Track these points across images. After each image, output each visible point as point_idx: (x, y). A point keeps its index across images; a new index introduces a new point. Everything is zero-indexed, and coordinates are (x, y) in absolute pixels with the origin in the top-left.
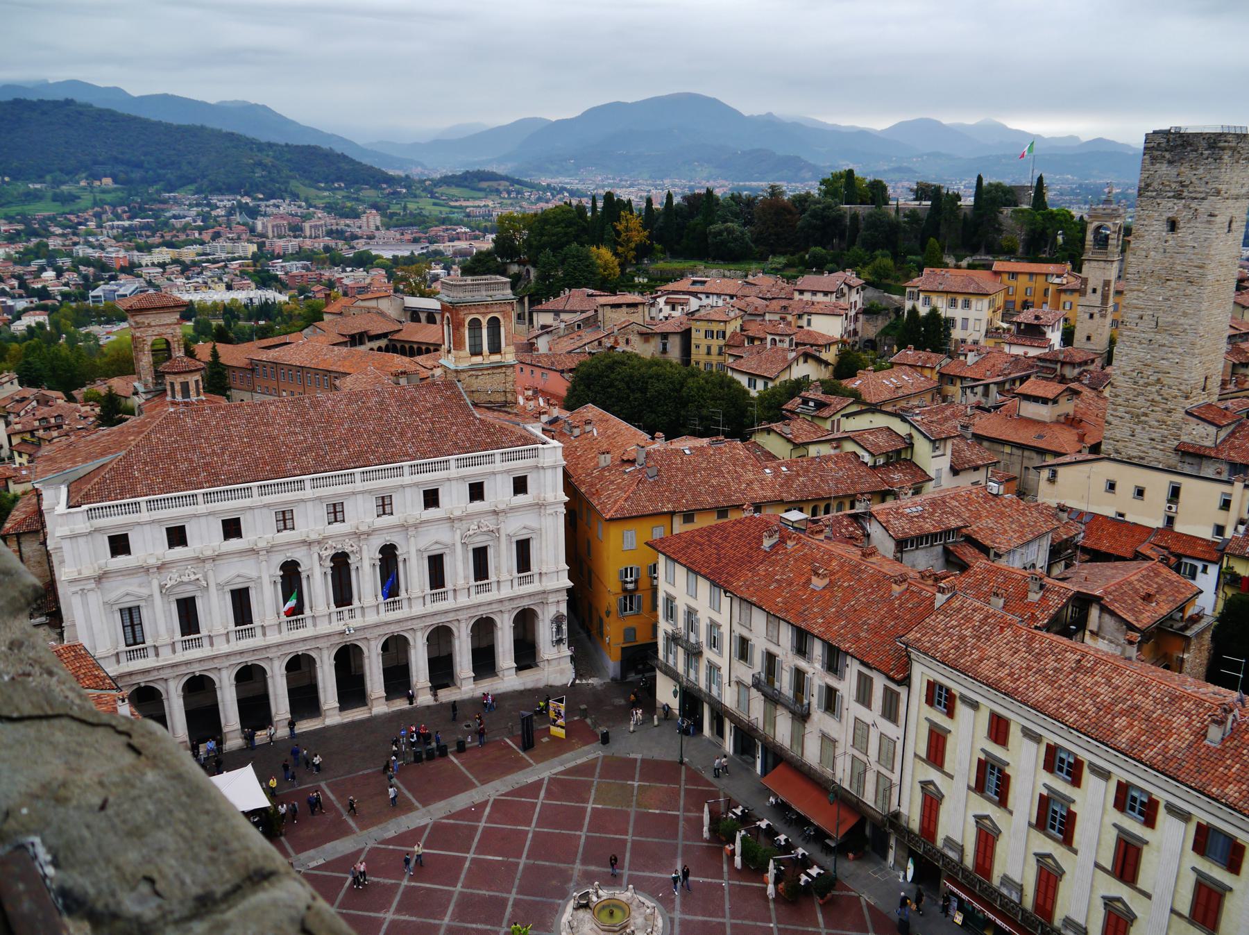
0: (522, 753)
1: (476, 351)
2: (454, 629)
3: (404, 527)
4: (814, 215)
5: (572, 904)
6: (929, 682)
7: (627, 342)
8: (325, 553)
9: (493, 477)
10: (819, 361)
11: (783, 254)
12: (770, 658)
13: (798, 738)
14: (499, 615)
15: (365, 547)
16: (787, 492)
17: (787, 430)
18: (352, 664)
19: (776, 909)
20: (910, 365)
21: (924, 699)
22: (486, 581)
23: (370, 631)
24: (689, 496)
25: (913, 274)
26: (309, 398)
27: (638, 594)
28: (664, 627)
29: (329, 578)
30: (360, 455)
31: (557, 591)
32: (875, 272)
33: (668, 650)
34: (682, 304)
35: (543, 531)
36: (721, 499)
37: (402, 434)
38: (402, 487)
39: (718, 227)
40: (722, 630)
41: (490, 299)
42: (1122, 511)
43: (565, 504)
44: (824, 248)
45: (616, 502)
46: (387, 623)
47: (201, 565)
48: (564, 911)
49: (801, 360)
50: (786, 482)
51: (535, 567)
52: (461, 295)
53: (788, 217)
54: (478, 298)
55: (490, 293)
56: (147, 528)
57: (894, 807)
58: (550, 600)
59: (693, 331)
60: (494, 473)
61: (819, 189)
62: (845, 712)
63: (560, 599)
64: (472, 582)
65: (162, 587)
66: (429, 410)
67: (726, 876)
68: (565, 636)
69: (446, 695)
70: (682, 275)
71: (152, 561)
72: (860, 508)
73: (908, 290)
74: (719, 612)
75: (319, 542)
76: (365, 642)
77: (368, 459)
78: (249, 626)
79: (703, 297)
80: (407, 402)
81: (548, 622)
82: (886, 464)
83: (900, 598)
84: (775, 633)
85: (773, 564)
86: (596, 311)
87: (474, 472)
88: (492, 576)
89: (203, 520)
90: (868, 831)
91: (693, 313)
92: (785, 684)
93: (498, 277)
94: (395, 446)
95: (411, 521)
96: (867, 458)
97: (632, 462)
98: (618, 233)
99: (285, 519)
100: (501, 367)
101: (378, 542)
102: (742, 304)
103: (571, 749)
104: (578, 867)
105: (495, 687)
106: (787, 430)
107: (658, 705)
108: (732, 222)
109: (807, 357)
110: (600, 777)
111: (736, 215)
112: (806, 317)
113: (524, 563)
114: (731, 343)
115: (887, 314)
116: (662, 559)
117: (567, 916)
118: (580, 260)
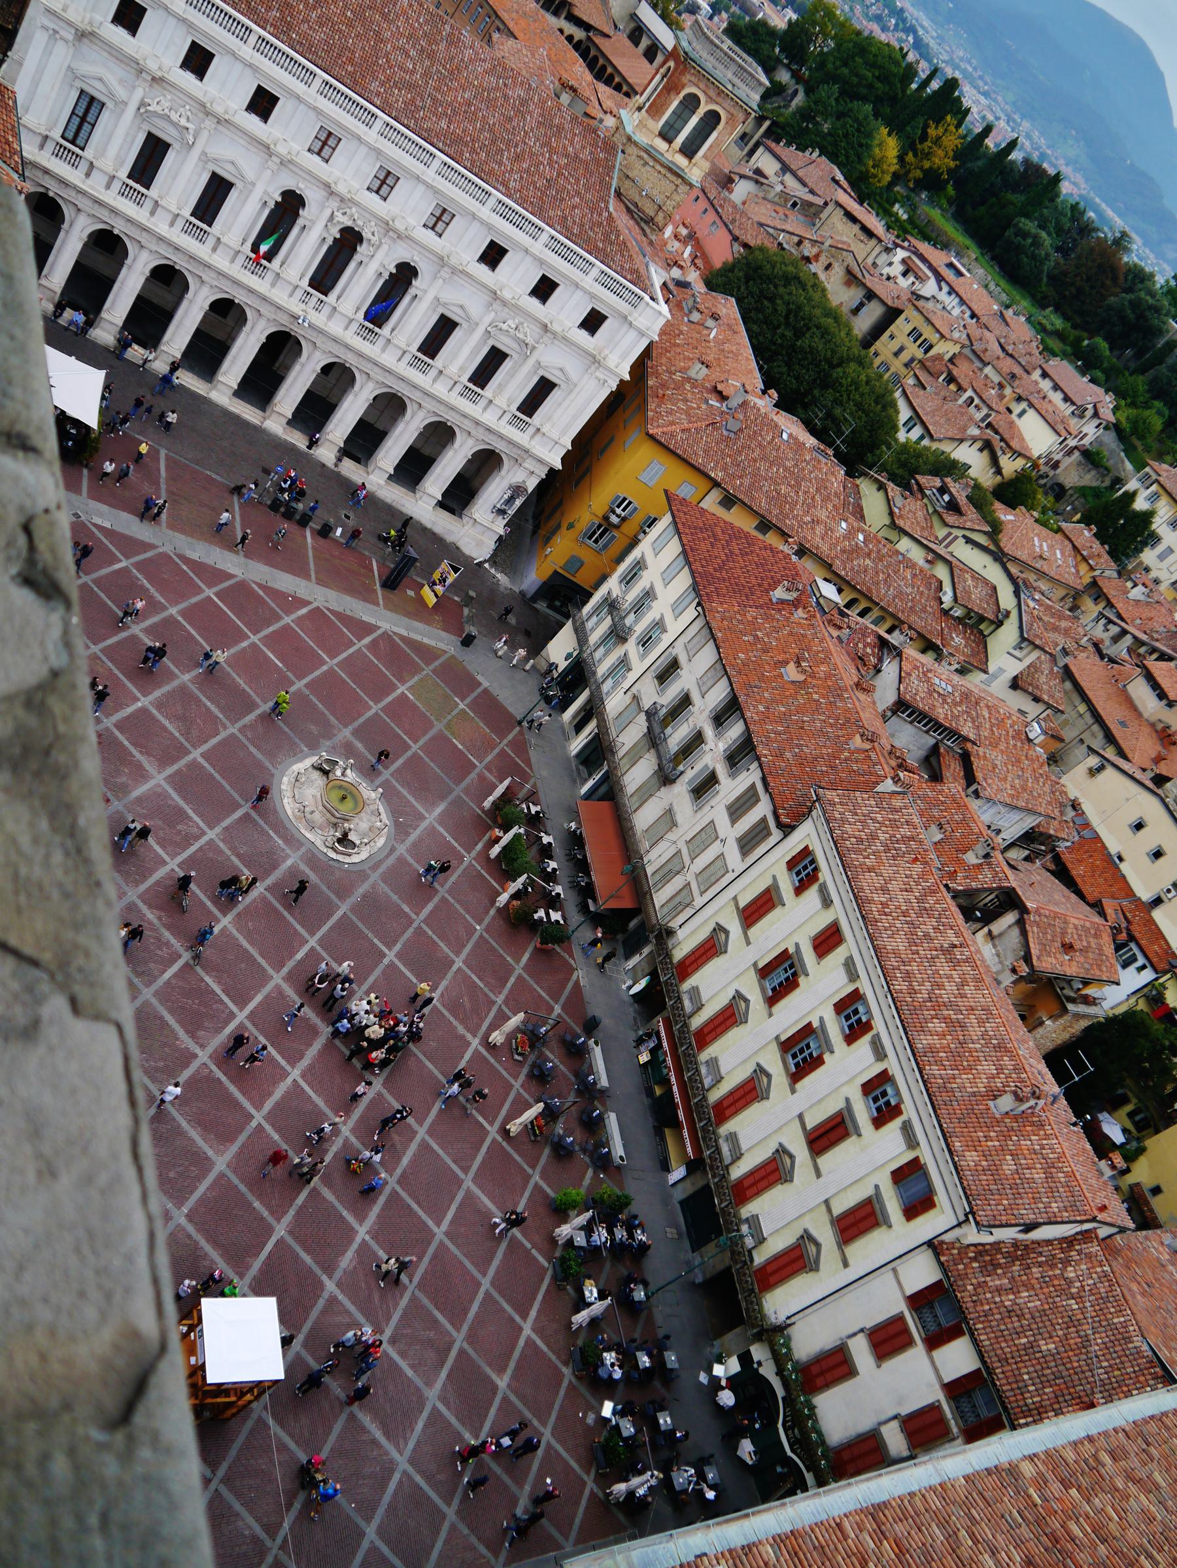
0: (378, 587)
1: (667, 135)
3: (442, 261)
4: (1136, 305)
5: (314, 759)
6: (807, 847)
7: (828, 267)
8: (339, 217)
9: (573, 288)
10: (995, 461)
11: (1066, 318)
12: (685, 701)
13: (645, 793)
14: (465, 435)
15: (385, 247)
16: (843, 562)
17: (899, 501)
18: (281, 358)
19: (494, 918)
20: (1074, 547)
21: (788, 858)
22: (478, 390)
23: (324, 339)
24: (747, 481)
25: (1169, 458)
26: (452, 27)
27: (615, 533)
28: (612, 585)
30: (457, 140)
31: (540, 461)
32: (1134, 422)
33: (597, 610)
34: (917, 277)
36: (775, 512)
37: (518, 158)
38: (474, 216)
39: (1029, 225)
40: (664, 636)
41: (730, 87)
42: (1124, 856)
43: (622, 381)
44: (1111, 349)
45: (672, 423)
46: (347, 347)
47: (201, 115)
48: (301, 760)
49: (978, 444)
50: (852, 552)
52: (705, 55)
53: (1108, 282)
54: (718, 74)
55: (736, 80)
56: (172, 21)
57: (674, 924)
58: (526, 465)
59: (903, 317)
60: (577, 286)
61: (1167, 281)
62: (707, 808)
64: (464, 379)
65: (143, 104)
66: (567, 156)
67: (474, 853)
68: (511, 512)
69: (349, 469)
70: (944, 244)
71: (152, 65)
72: (895, 639)
73: (1147, 469)
74: (676, 618)
75: (342, 200)
76: (311, 347)
77: (462, 154)
78: (205, 227)
79: (945, 289)
80: (551, 127)
82: (959, 620)
83: (852, 753)
84: (709, 684)
85: (767, 618)
86: (826, 204)
87: (559, 268)
88: (488, 392)
89: (239, 66)
90: (633, 924)
91: (919, 297)
92: (677, 736)
93: (760, 69)
94: (500, 163)
95: (453, 261)
96: (947, 598)
97: (723, 397)
98: (924, 137)
99: (326, 143)
100: (678, 176)
101: (403, 253)
102: (976, 332)
103: (428, 623)
104: (346, 733)
105: (404, 502)
106: (899, 501)
107: (543, 653)
108: (1049, 234)
109: (987, 446)
110: (434, 671)
111: (1060, 231)
112: (1024, 405)
113: (531, 404)
114: (928, 364)
115: (1103, 476)
116: (667, 519)
117: (299, 767)
118: (858, 130)
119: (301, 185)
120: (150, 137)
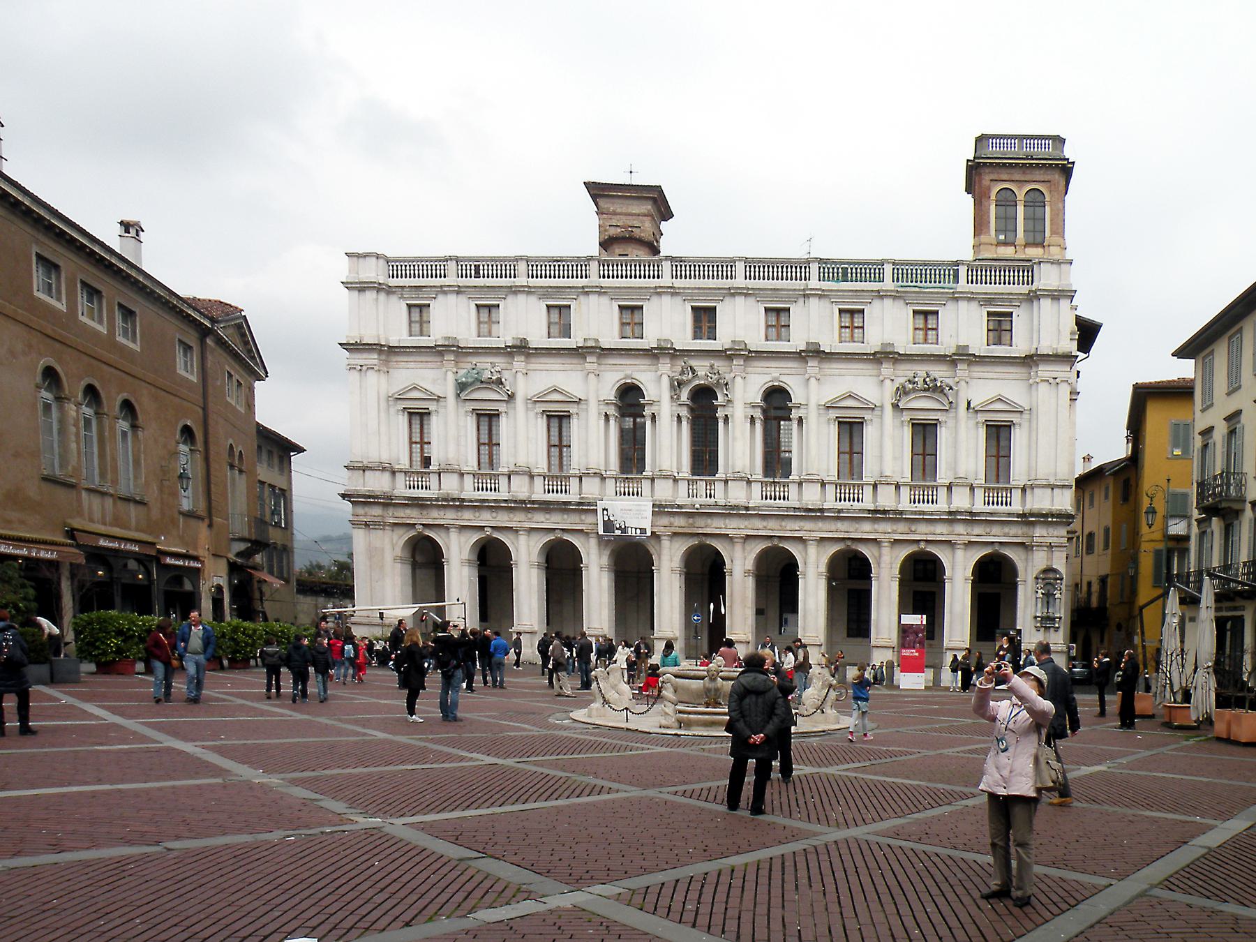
29: (685, 426)
88: (943, 476)
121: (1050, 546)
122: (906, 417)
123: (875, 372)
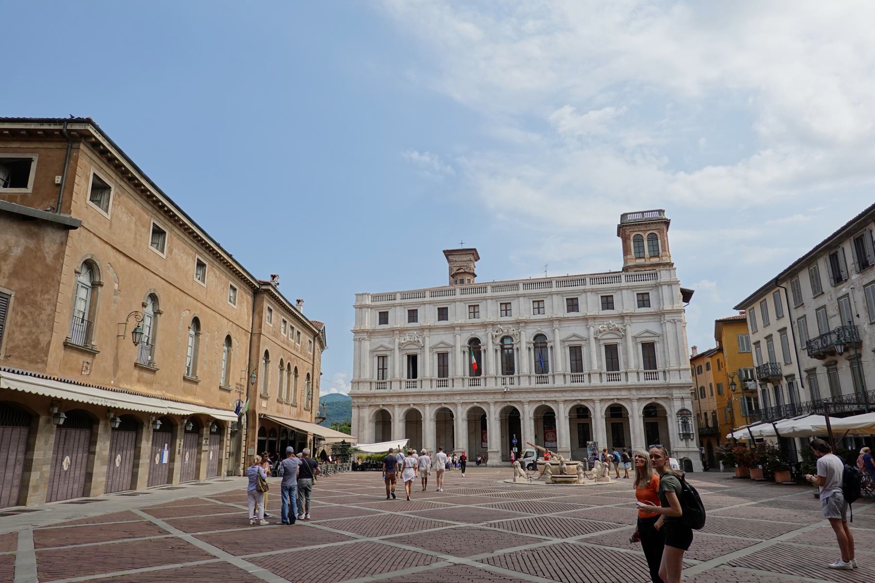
2: (591, 410)
3: (551, 321)
15: (522, 332)
31: (681, 387)
35: (665, 335)
51: (660, 366)
63: (684, 395)
65: (400, 344)
78: (445, 378)
81: (674, 416)
88: (622, 368)
99: (474, 310)
119: (473, 333)
120: (409, 356)
121: (682, 399)
122: (602, 342)
123: (585, 324)
